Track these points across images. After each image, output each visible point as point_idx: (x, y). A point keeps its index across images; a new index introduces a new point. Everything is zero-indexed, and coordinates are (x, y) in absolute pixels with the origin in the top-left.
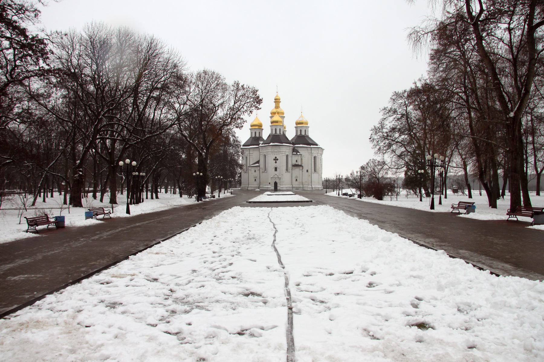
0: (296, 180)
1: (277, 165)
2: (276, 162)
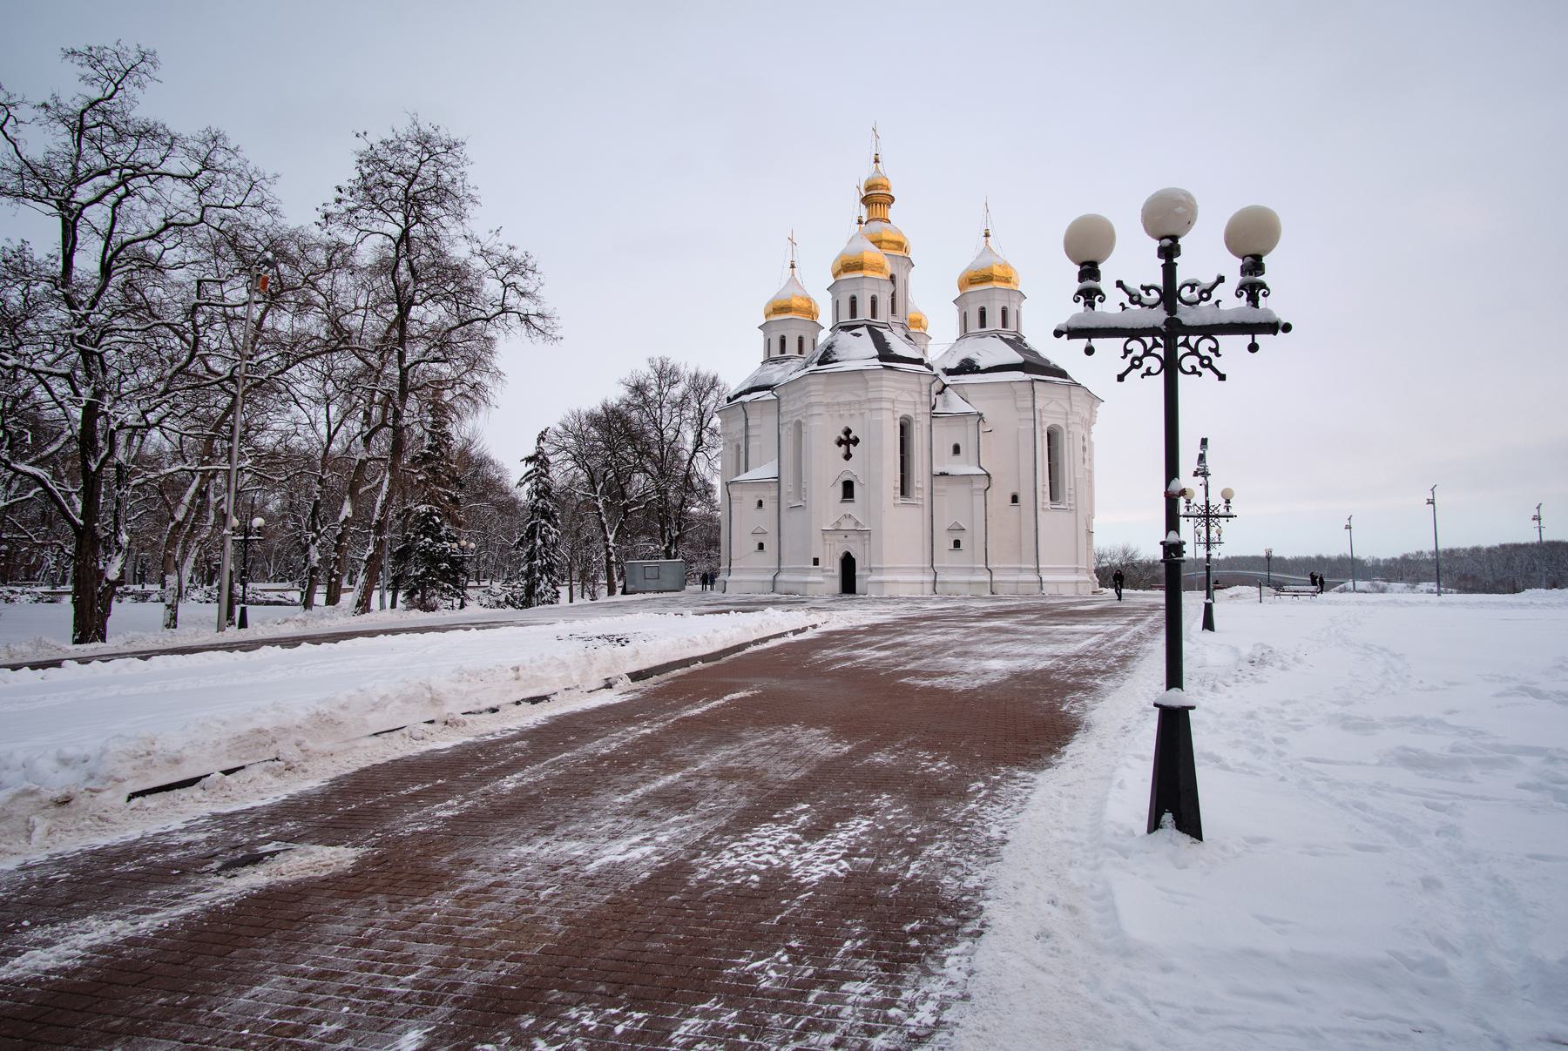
0: (957, 544)
1: (853, 469)
2: (848, 456)
